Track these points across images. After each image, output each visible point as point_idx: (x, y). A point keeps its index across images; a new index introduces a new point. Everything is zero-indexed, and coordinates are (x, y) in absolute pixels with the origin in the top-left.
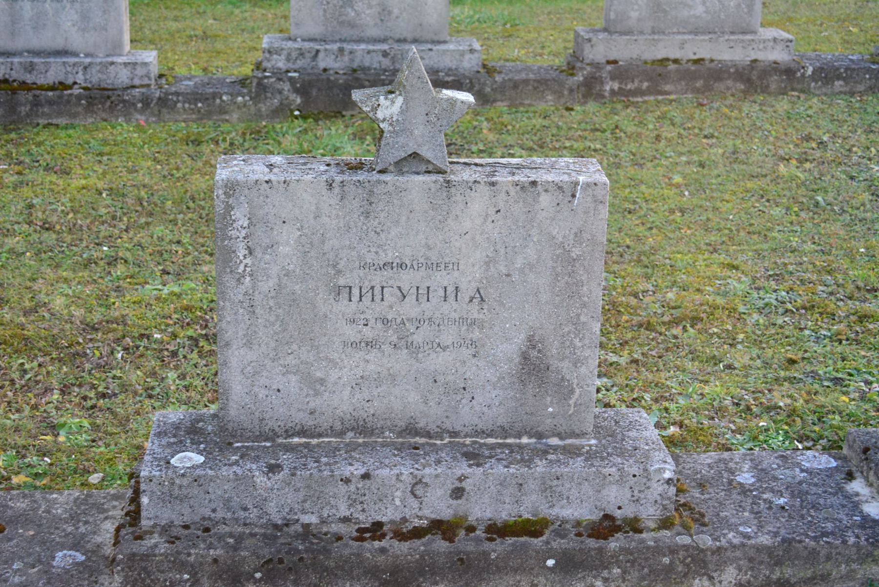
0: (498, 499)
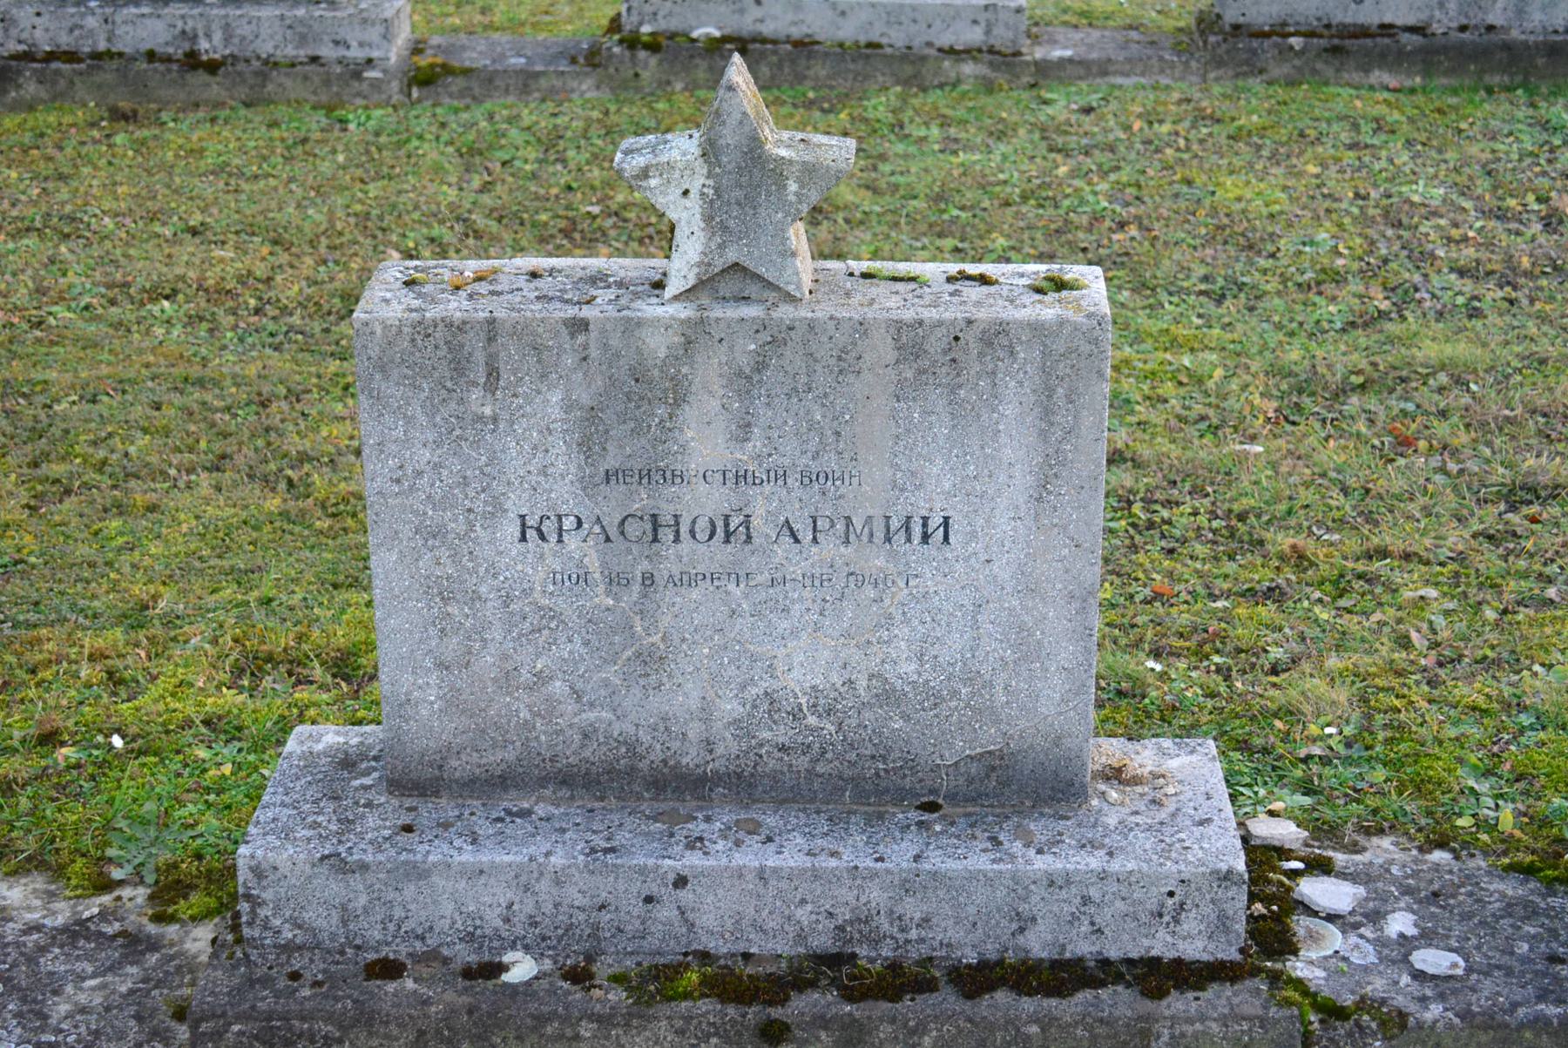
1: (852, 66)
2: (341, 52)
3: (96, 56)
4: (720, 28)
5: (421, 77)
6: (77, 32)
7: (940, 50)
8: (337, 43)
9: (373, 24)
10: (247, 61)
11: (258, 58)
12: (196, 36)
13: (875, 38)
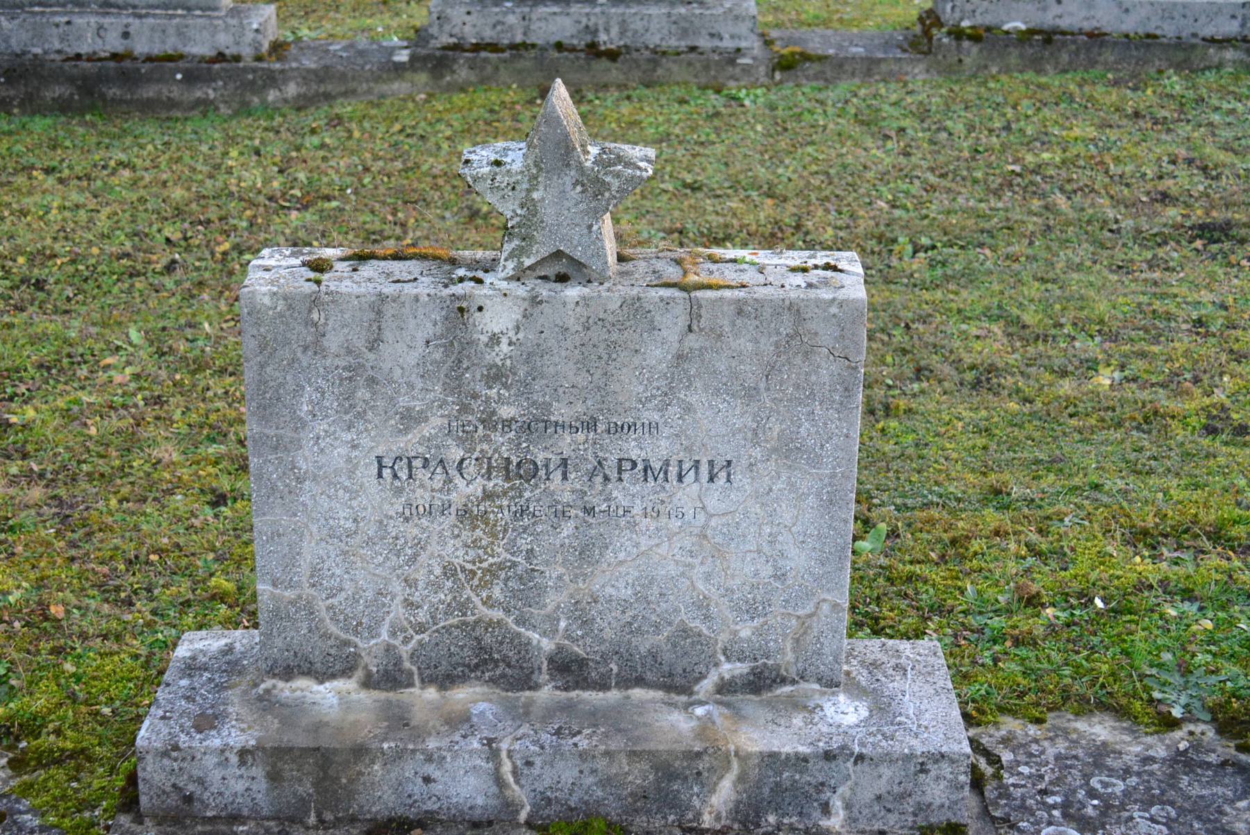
0: (151, 40)
1: (1135, 53)
2: (716, 43)
3: (513, 47)
4: (1025, 23)
5: (784, 63)
6: (499, 28)
7: (1204, 39)
8: (712, 35)
9: (744, 20)
10: (638, 50)
11: (647, 48)
12: (597, 31)
13: (1152, 31)
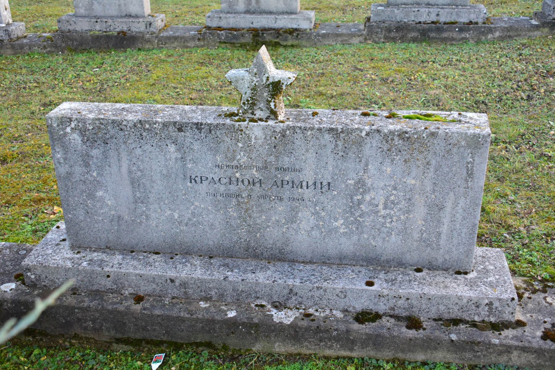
0: (447, 17)
